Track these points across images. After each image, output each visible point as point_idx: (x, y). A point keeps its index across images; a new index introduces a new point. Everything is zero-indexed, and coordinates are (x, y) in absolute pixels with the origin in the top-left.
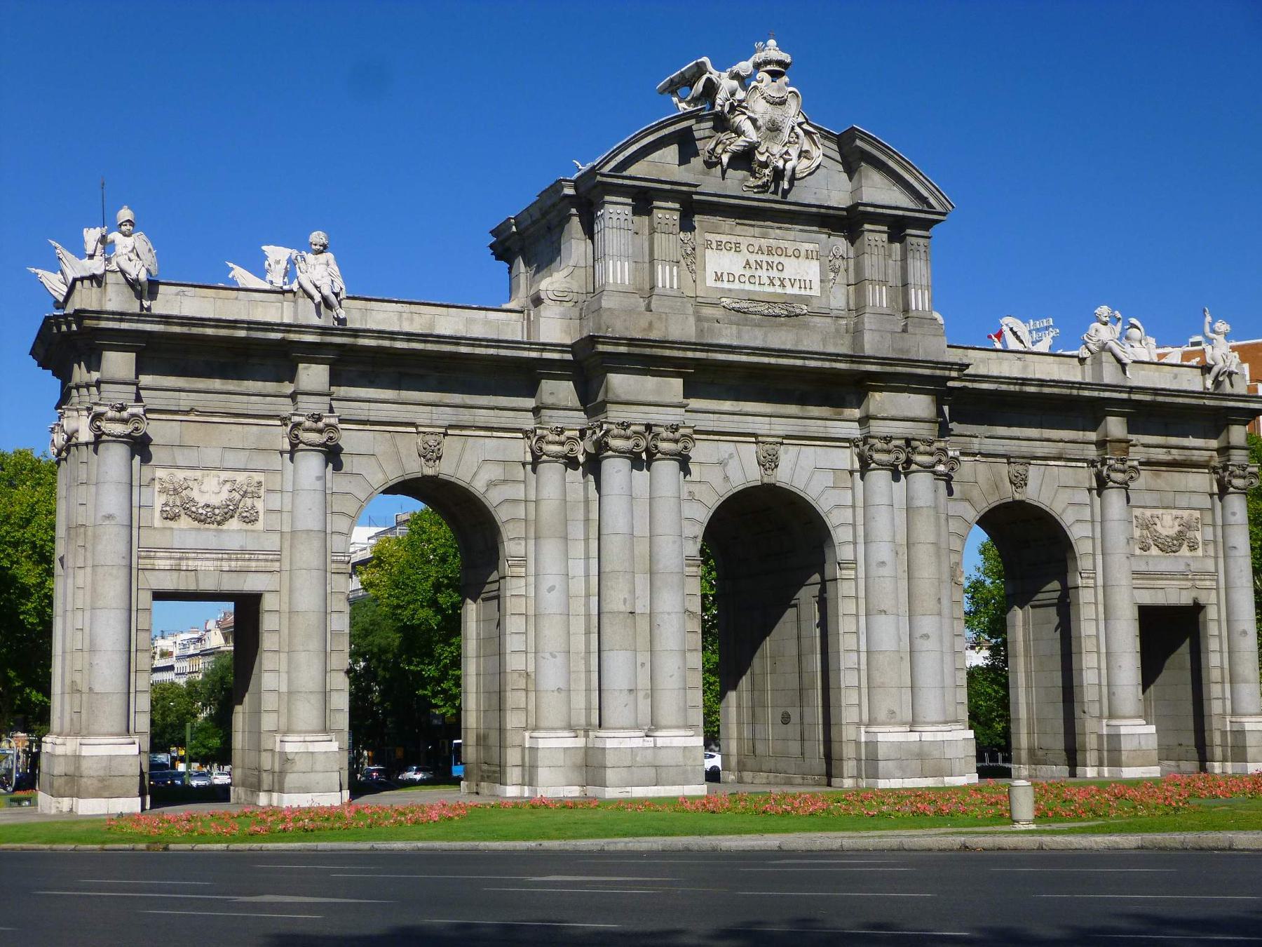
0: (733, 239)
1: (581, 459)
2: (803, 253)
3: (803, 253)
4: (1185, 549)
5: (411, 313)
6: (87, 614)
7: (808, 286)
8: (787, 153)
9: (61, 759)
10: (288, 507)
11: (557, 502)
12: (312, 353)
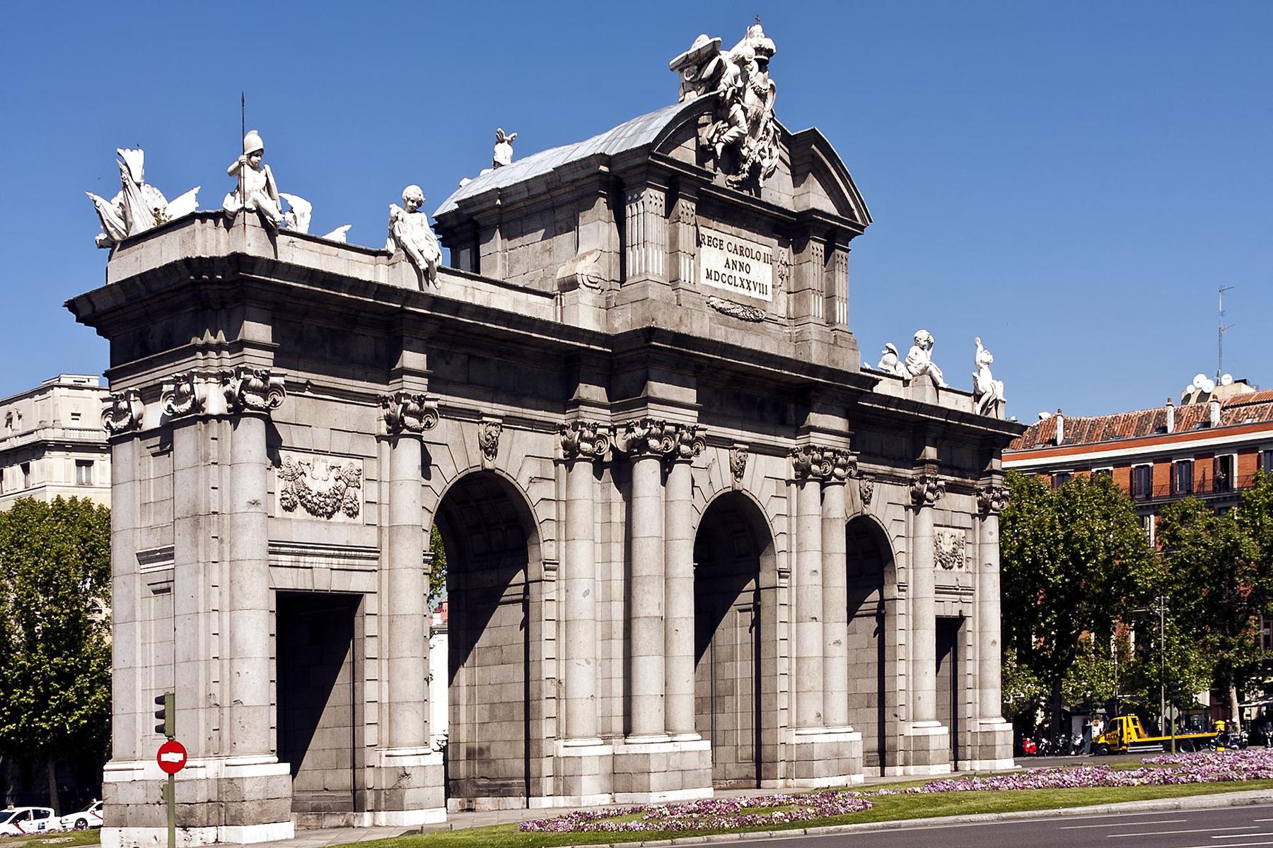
1: (608, 457)
5: (473, 288)
6: (226, 616)
9: (203, 784)
10: (386, 500)
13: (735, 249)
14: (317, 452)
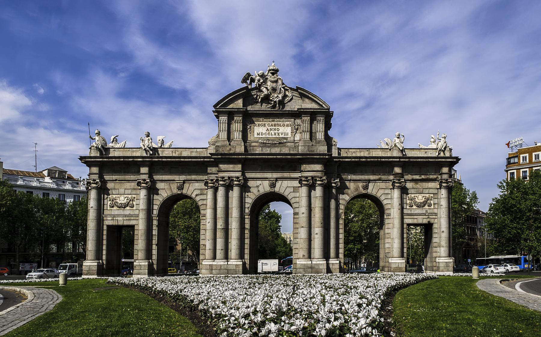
0: (263, 123)
2: (286, 125)
3: (286, 125)
4: (427, 206)
7: (287, 135)
8: (278, 96)
11: (211, 199)
12: (143, 164)
13: (272, 125)
14: (121, 194)
